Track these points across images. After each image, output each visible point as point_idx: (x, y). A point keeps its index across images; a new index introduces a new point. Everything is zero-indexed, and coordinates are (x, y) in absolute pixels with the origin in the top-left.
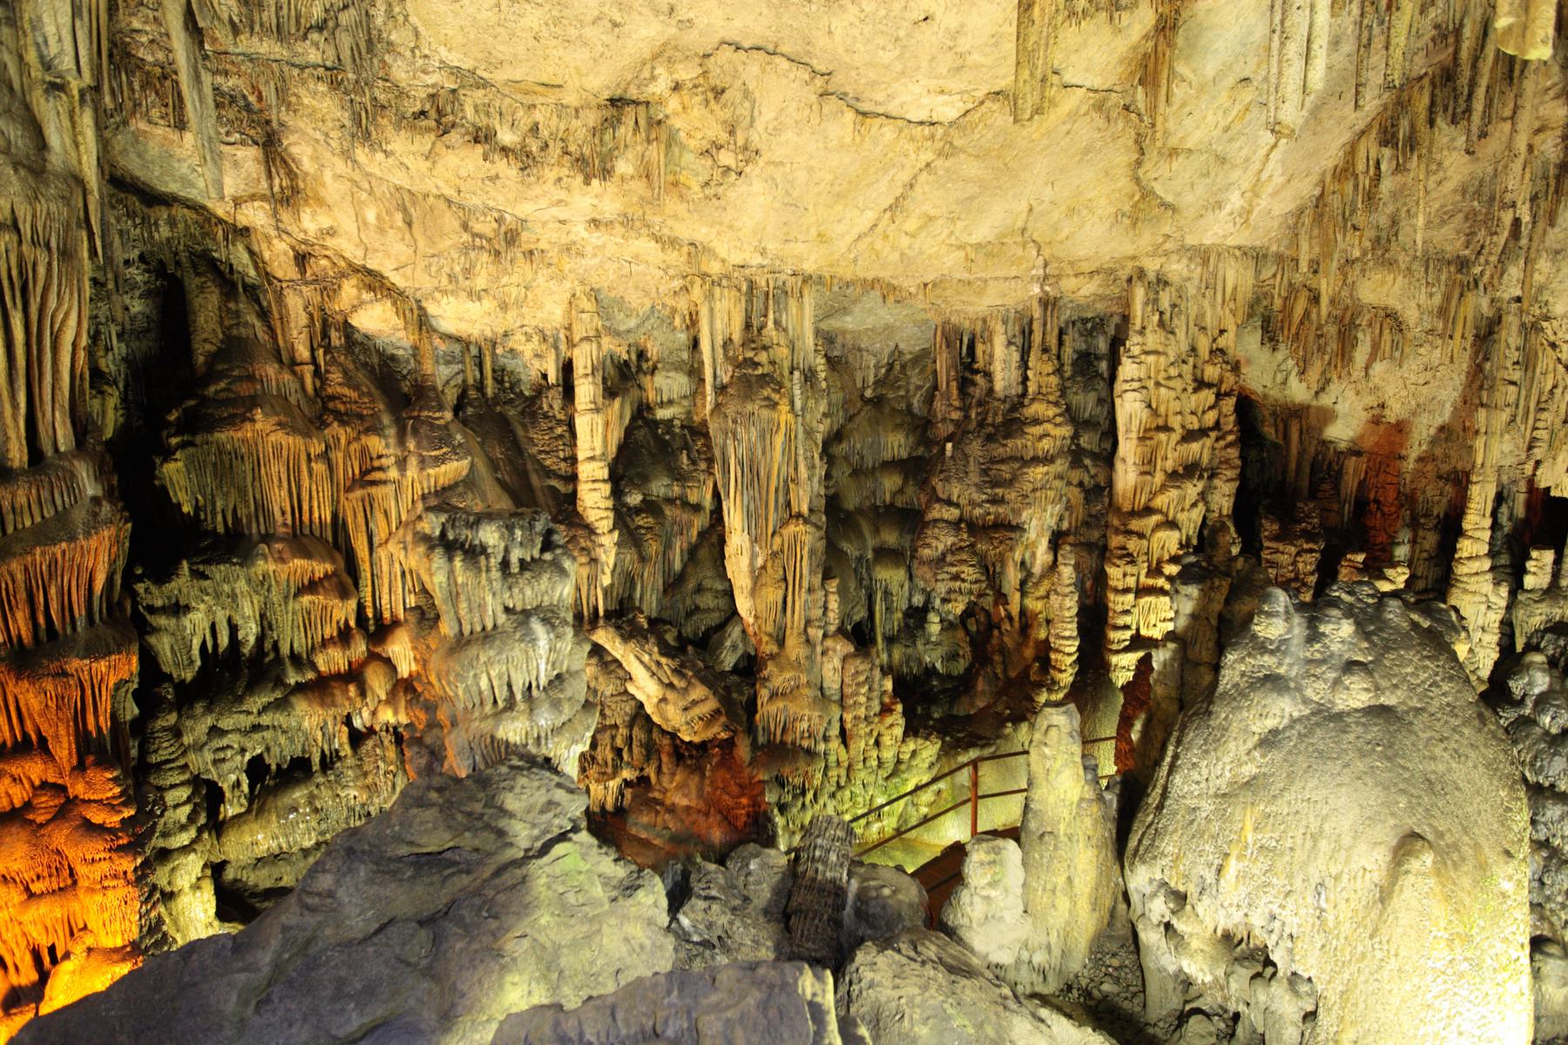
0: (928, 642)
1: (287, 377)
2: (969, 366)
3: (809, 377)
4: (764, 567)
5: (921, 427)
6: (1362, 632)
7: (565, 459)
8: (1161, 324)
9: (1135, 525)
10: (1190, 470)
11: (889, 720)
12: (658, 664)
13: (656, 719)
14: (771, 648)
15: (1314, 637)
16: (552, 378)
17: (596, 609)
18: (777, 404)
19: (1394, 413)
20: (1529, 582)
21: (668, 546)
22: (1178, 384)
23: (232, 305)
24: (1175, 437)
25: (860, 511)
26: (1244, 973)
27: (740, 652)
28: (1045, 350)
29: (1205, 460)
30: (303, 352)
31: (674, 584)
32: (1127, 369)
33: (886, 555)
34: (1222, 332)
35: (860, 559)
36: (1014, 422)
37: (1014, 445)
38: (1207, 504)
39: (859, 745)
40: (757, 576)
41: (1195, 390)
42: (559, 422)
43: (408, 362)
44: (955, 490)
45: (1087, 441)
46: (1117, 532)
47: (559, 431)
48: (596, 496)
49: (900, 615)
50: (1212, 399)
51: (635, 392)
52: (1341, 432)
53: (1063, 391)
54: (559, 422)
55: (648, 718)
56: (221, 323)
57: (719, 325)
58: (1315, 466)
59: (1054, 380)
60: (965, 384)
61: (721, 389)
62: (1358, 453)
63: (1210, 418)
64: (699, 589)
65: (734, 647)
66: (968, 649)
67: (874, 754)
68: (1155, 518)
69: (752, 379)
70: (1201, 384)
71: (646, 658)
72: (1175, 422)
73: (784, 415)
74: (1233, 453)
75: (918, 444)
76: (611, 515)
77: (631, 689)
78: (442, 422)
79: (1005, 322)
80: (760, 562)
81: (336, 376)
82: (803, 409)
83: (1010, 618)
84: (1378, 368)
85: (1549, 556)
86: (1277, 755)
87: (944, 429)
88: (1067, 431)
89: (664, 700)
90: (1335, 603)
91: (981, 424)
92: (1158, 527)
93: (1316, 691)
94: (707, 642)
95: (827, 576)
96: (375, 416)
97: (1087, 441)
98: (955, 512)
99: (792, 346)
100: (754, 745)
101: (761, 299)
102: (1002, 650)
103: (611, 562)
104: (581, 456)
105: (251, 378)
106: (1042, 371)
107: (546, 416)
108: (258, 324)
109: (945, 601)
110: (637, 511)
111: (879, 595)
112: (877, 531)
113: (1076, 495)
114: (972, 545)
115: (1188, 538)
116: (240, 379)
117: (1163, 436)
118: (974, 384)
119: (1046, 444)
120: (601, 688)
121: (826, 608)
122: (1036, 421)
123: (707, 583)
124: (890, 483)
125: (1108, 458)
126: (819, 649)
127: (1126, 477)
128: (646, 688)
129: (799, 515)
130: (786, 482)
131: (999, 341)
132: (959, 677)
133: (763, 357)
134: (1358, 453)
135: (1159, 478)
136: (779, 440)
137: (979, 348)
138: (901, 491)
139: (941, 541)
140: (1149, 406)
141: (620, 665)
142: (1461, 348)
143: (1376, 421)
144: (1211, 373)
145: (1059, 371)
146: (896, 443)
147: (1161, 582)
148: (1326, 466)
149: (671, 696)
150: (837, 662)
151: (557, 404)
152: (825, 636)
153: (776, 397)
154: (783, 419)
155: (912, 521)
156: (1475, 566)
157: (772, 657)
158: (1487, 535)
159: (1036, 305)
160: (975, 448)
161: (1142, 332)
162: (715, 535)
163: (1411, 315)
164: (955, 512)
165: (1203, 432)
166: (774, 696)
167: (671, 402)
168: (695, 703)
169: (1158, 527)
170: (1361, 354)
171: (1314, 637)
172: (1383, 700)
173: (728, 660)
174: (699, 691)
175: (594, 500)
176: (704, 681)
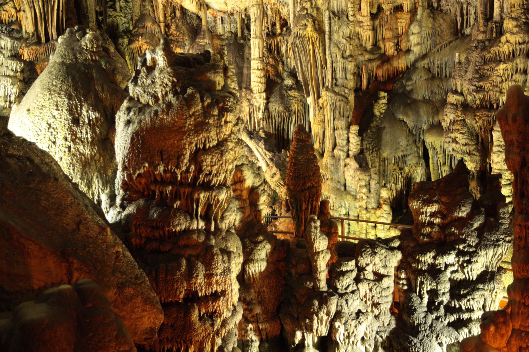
1: (155, 27)
12: (265, 154)
23: (144, 3)
25: (426, 101)
30: (162, 19)
43: (211, 23)
56: (140, 10)
71: (260, 150)
78: (203, 44)
81: (173, 27)
96: (183, 41)
98: (460, 98)
105: (143, 27)
108: (150, 9)
110: (290, 88)
116: (140, 27)
121: (348, 141)
139: (448, 117)
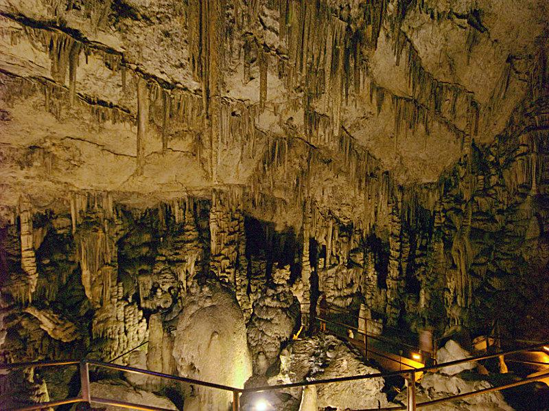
0: (158, 298)
2: (169, 214)
3: (111, 221)
4: (95, 281)
5: (155, 233)
6: (211, 290)
7: (17, 250)
8: (221, 203)
9: (216, 259)
10: (231, 243)
11: (141, 324)
12: (53, 317)
13: (52, 336)
14: (99, 306)
15: (201, 291)
16: (12, 222)
17: (28, 300)
18: (98, 230)
19: (289, 224)
20: (320, 266)
21: (60, 276)
22: (227, 220)
24: (226, 234)
26: (192, 371)
27: (87, 310)
28: (189, 210)
29: (236, 239)
31: (62, 289)
32: (212, 216)
33: (143, 272)
34: (239, 205)
35: (134, 275)
36: (182, 231)
37: (182, 237)
38: (238, 252)
39: (130, 334)
40: (92, 284)
41: (232, 221)
42: (15, 237)
44: (164, 252)
45: (204, 235)
46: (212, 261)
47: (15, 240)
48: (29, 262)
49: (149, 291)
50: (237, 223)
51: (48, 225)
52: (279, 229)
53: (196, 221)
54: (15, 237)
55: (49, 336)
57: (77, 206)
58: (274, 239)
59: (192, 219)
60: (167, 220)
61: (78, 226)
62: (283, 234)
63: (237, 228)
64: (73, 289)
65: (85, 308)
66: (171, 299)
67: (137, 336)
68: (222, 257)
69: (90, 222)
70: (233, 219)
71: (48, 315)
72: (226, 230)
73: (100, 233)
74: (244, 237)
75: (153, 237)
76: (35, 268)
77: (42, 327)
79: (178, 202)
80: (94, 279)
82: (108, 231)
83: (183, 288)
84: (284, 213)
85: (323, 260)
86: (192, 319)
87: (160, 234)
88: (196, 234)
89: (55, 329)
90: (206, 283)
91: (172, 232)
92: (223, 259)
93: (201, 303)
94: (74, 307)
95: (118, 282)
97: (204, 235)
98: (164, 258)
99: (104, 212)
100: (91, 340)
101: (92, 199)
102: (180, 298)
103: (35, 284)
104: (23, 249)
106: (189, 217)
107: (9, 236)
109: (163, 285)
110: (47, 265)
111: (141, 286)
112: (140, 265)
113: (200, 250)
114: (170, 268)
115: (233, 262)
117: (223, 234)
118: (170, 219)
119: (190, 237)
120: (29, 328)
121: (118, 292)
122: (188, 231)
123: (76, 287)
124: (145, 250)
125: (209, 239)
126: (116, 305)
127: (213, 246)
128: (48, 326)
129: (107, 264)
130: (102, 254)
131: (177, 207)
132: (169, 308)
133: (93, 216)
134: (283, 234)
135: (222, 245)
136: (99, 241)
137: (172, 209)
138: (148, 252)
139: (160, 267)
140: (218, 226)
141: (37, 319)
142: (298, 208)
143: (286, 226)
144: (236, 216)
145: (195, 216)
146: (147, 238)
147: (225, 274)
148: (276, 237)
149: (58, 327)
150: (122, 308)
151: (14, 231)
152: (118, 300)
153: (98, 228)
154: (100, 235)
155: (151, 261)
156: (306, 263)
157: (98, 309)
158: (308, 255)
159: (186, 198)
160: (170, 239)
161: (215, 206)
162: (79, 271)
163: (288, 200)
164: (164, 258)
165: (235, 232)
166: (99, 322)
167: (63, 228)
168: (67, 328)
169: (223, 259)
170: (278, 210)
171: (201, 291)
172: (214, 304)
173: (83, 312)
174: (69, 324)
175: (28, 264)
176: (72, 321)
